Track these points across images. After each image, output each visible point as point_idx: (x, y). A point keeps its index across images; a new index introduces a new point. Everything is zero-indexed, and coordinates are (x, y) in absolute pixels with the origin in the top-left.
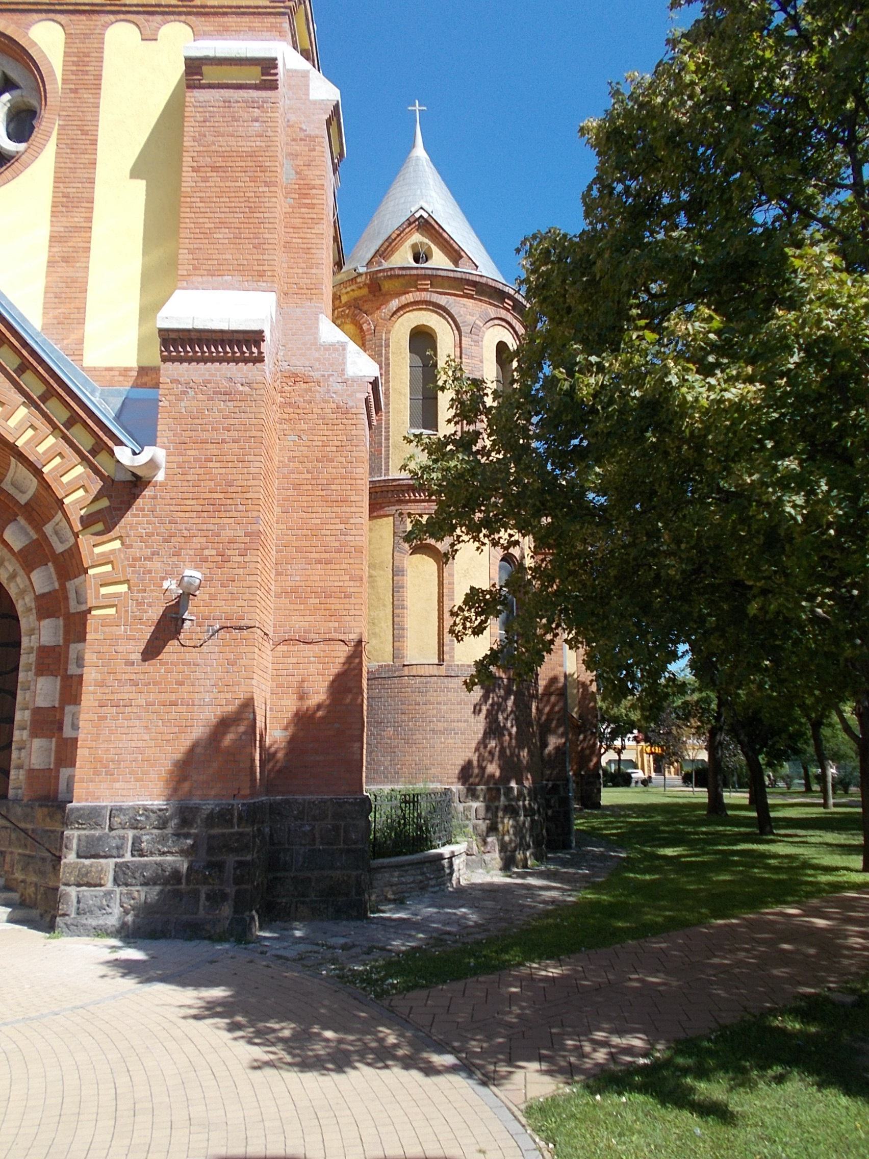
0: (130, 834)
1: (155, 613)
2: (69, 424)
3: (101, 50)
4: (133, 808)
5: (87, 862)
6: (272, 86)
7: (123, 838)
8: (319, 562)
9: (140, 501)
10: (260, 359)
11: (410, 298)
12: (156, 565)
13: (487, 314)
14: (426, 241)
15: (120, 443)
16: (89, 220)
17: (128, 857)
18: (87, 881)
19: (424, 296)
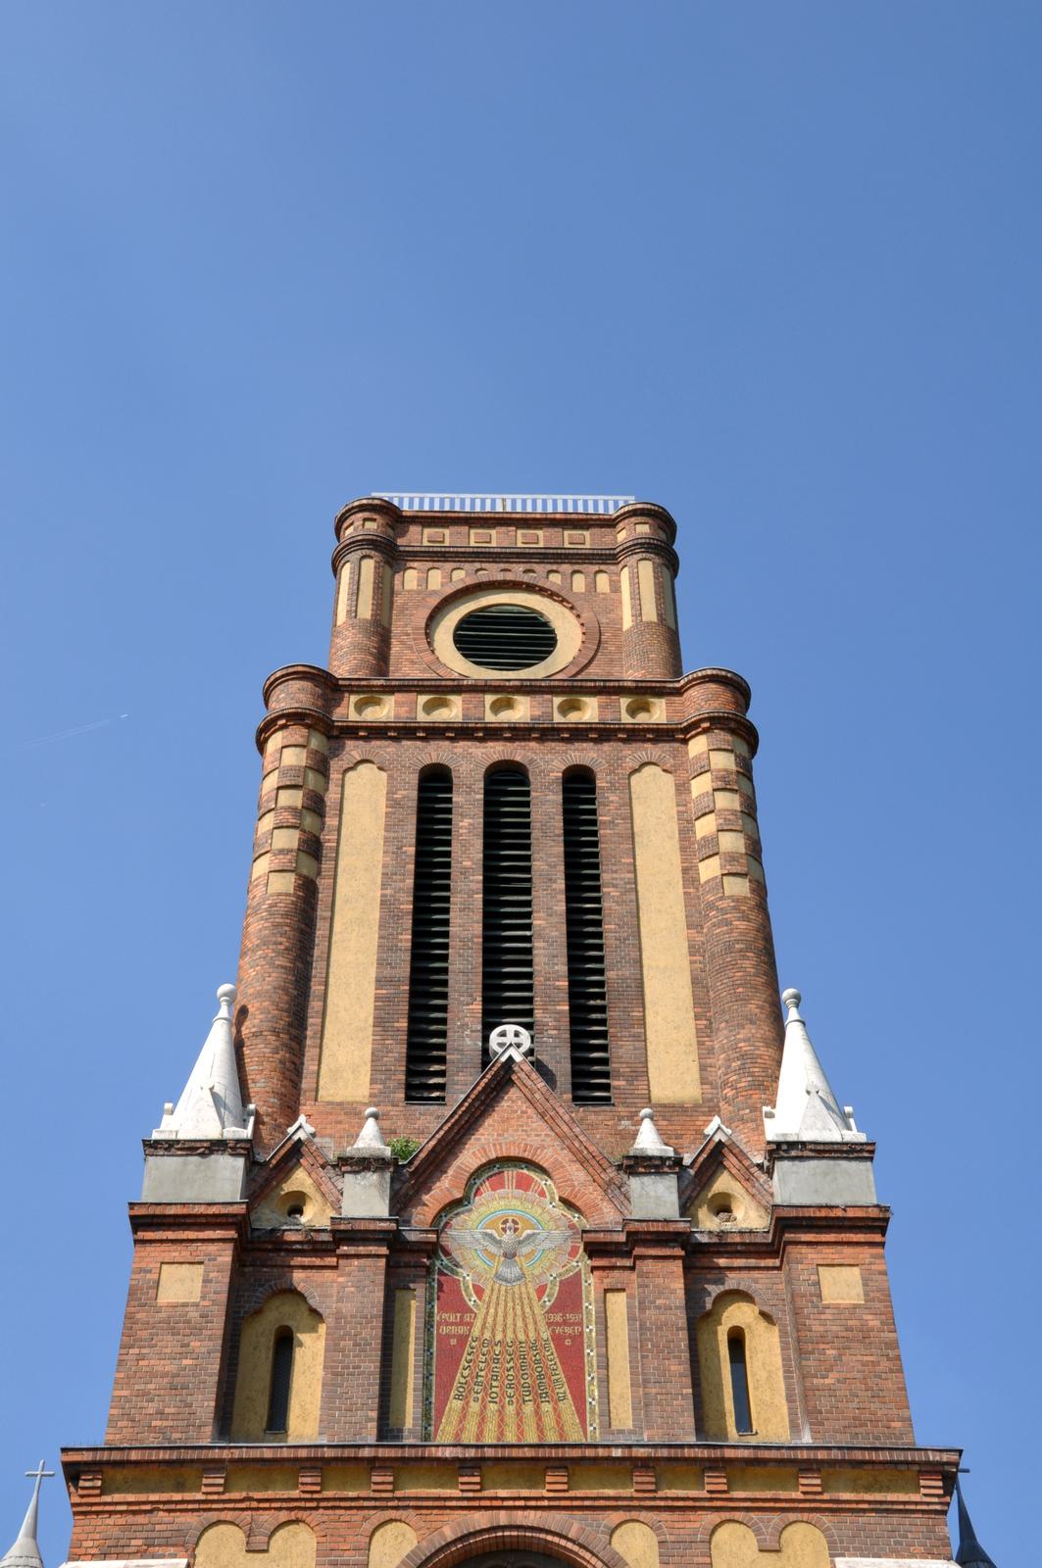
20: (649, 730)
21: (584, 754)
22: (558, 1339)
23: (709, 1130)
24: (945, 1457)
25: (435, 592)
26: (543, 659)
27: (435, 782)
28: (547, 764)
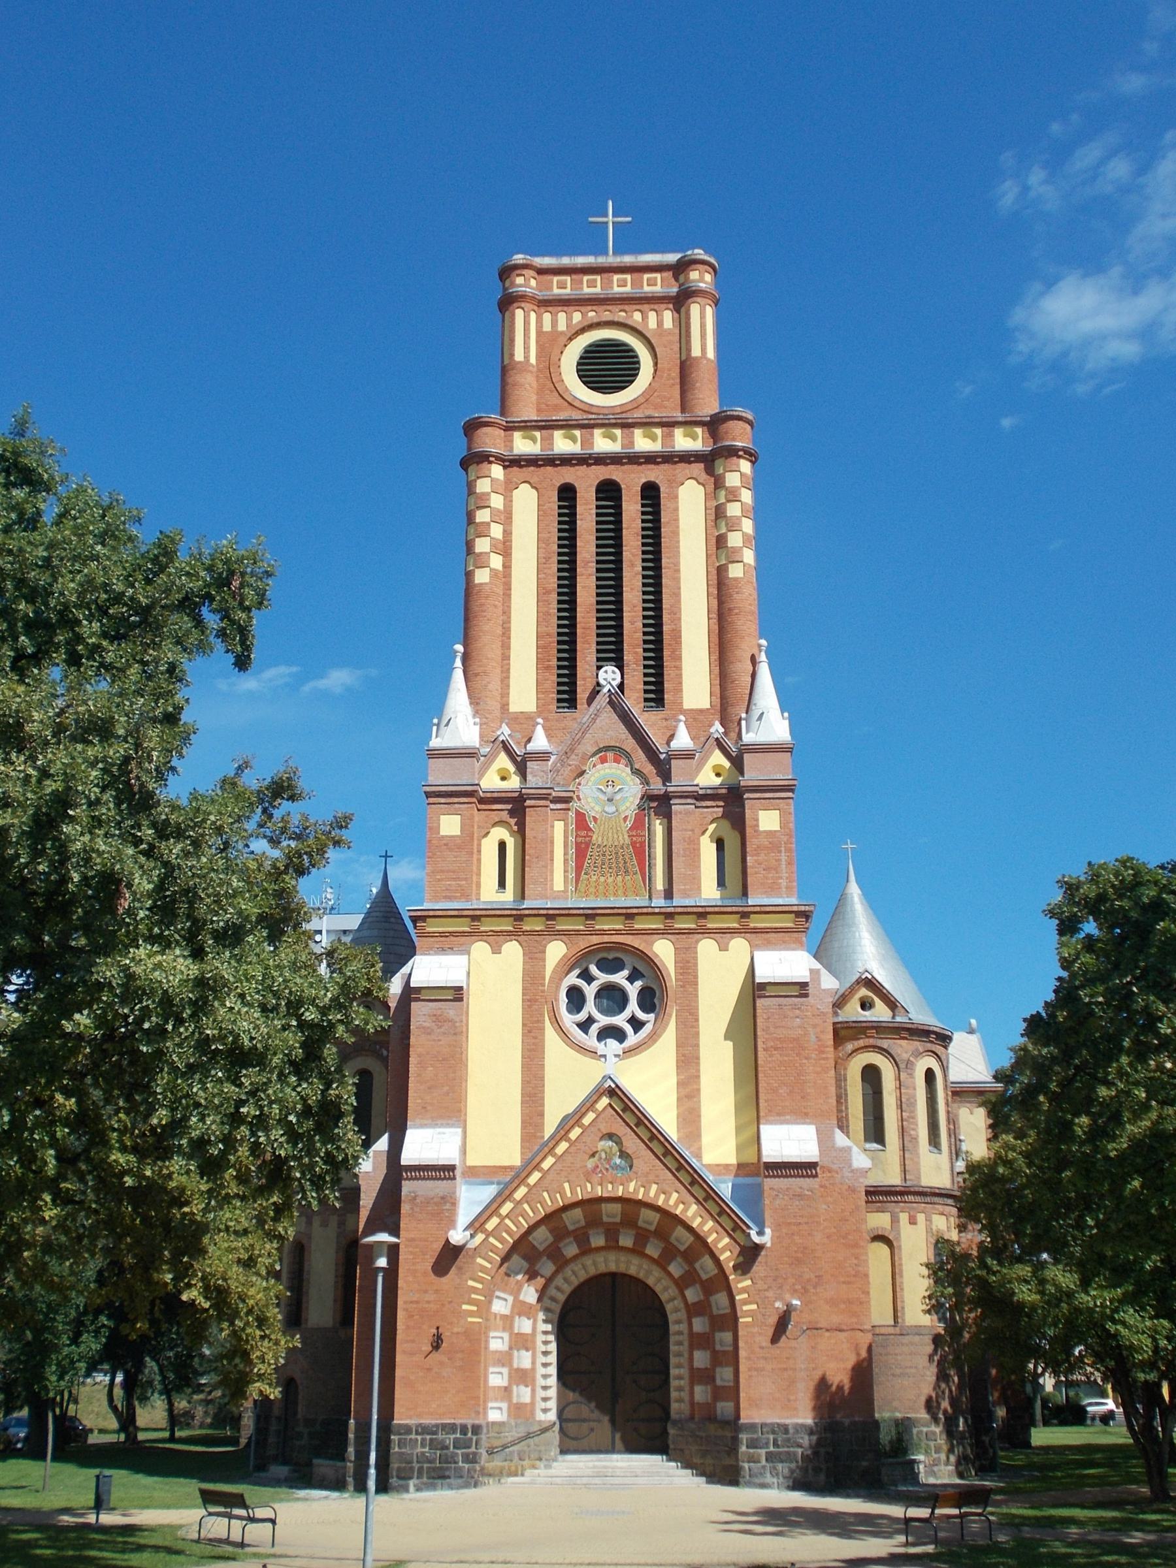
0: (771, 1437)
1: (773, 1320)
2: (720, 1214)
3: (696, 958)
4: (772, 1424)
5: (751, 1451)
6: (806, 996)
7: (768, 1439)
8: (844, 1283)
9: (760, 1259)
10: (816, 1176)
11: (861, 1043)
12: (770, 1294)
13: (917, 1050)
14: (871, 994)
15: (749, 1227)
16: (698, 1071)
17: (772, 1449)
18: (753, 1459)
19: (871, 1041)
20: (691, 456)
21: (651, 474)
22: (633, 844)
23: (712, 730)
24: (807, 908)
25: (562, 333)
26: (632, 382)
27: (567, 494)
28: (631, 481)
